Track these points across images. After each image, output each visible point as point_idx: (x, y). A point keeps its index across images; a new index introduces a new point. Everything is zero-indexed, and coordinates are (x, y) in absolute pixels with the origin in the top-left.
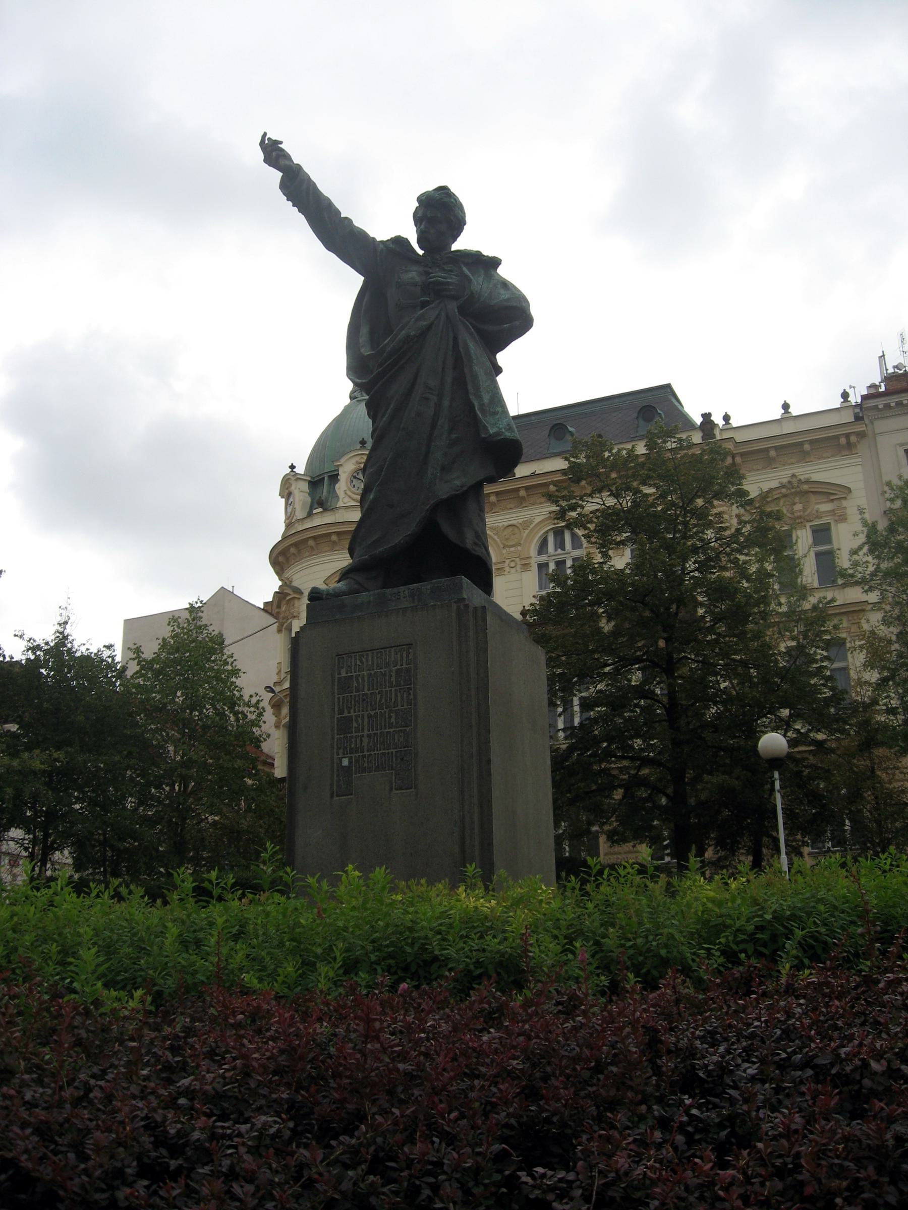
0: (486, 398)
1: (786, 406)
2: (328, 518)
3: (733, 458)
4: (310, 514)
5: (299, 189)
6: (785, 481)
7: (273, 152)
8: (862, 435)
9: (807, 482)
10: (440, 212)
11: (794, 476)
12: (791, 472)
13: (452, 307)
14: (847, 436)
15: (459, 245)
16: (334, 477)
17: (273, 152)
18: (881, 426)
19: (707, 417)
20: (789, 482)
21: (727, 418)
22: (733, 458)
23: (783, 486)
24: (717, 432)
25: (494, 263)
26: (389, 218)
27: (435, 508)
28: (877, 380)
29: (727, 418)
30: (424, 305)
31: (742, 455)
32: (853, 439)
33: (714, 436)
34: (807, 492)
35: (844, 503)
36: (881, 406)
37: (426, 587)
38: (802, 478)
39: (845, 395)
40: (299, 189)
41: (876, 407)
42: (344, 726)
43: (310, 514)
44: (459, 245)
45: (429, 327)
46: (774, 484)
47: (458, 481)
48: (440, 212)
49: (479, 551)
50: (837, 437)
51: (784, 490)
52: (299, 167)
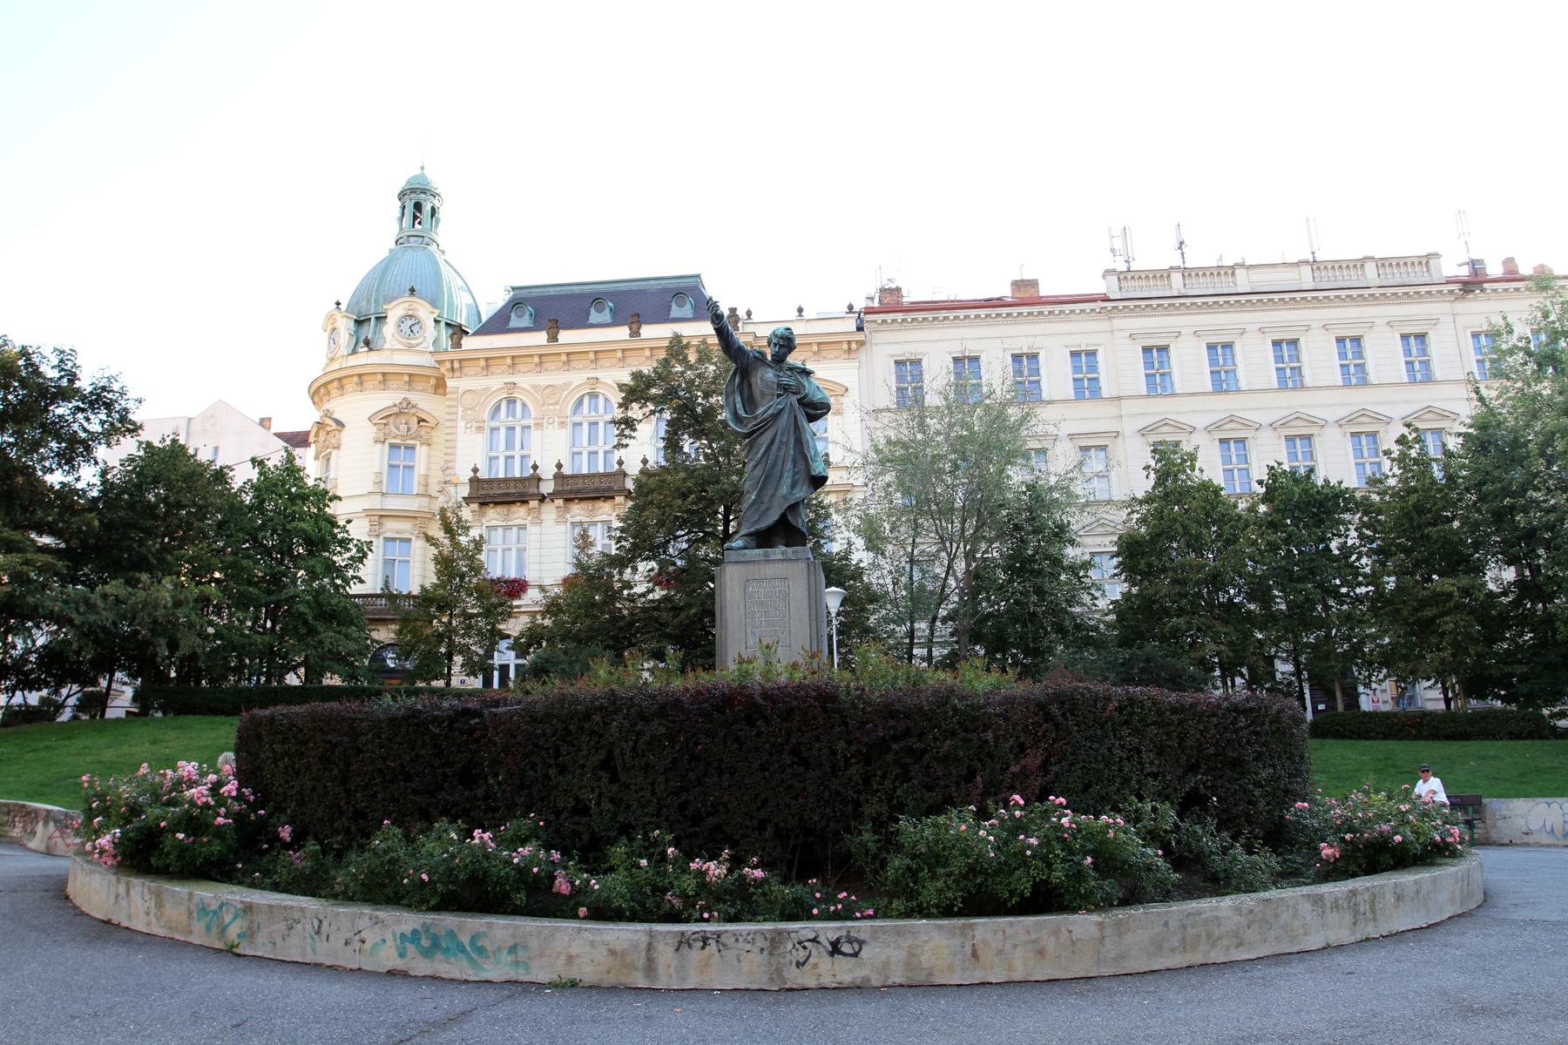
1: (800, 310)
2: (374, 358)
4: (354, 352)
8: (861, 344)
13: (794, 399)
16: (381, 319)
18: (878, 338)
19: (733, 310)
21: (749, 314)
29: (749, 314)
32: (854, 346)
37: (790, 550)
39: (851, 308)
43: (354, 352)
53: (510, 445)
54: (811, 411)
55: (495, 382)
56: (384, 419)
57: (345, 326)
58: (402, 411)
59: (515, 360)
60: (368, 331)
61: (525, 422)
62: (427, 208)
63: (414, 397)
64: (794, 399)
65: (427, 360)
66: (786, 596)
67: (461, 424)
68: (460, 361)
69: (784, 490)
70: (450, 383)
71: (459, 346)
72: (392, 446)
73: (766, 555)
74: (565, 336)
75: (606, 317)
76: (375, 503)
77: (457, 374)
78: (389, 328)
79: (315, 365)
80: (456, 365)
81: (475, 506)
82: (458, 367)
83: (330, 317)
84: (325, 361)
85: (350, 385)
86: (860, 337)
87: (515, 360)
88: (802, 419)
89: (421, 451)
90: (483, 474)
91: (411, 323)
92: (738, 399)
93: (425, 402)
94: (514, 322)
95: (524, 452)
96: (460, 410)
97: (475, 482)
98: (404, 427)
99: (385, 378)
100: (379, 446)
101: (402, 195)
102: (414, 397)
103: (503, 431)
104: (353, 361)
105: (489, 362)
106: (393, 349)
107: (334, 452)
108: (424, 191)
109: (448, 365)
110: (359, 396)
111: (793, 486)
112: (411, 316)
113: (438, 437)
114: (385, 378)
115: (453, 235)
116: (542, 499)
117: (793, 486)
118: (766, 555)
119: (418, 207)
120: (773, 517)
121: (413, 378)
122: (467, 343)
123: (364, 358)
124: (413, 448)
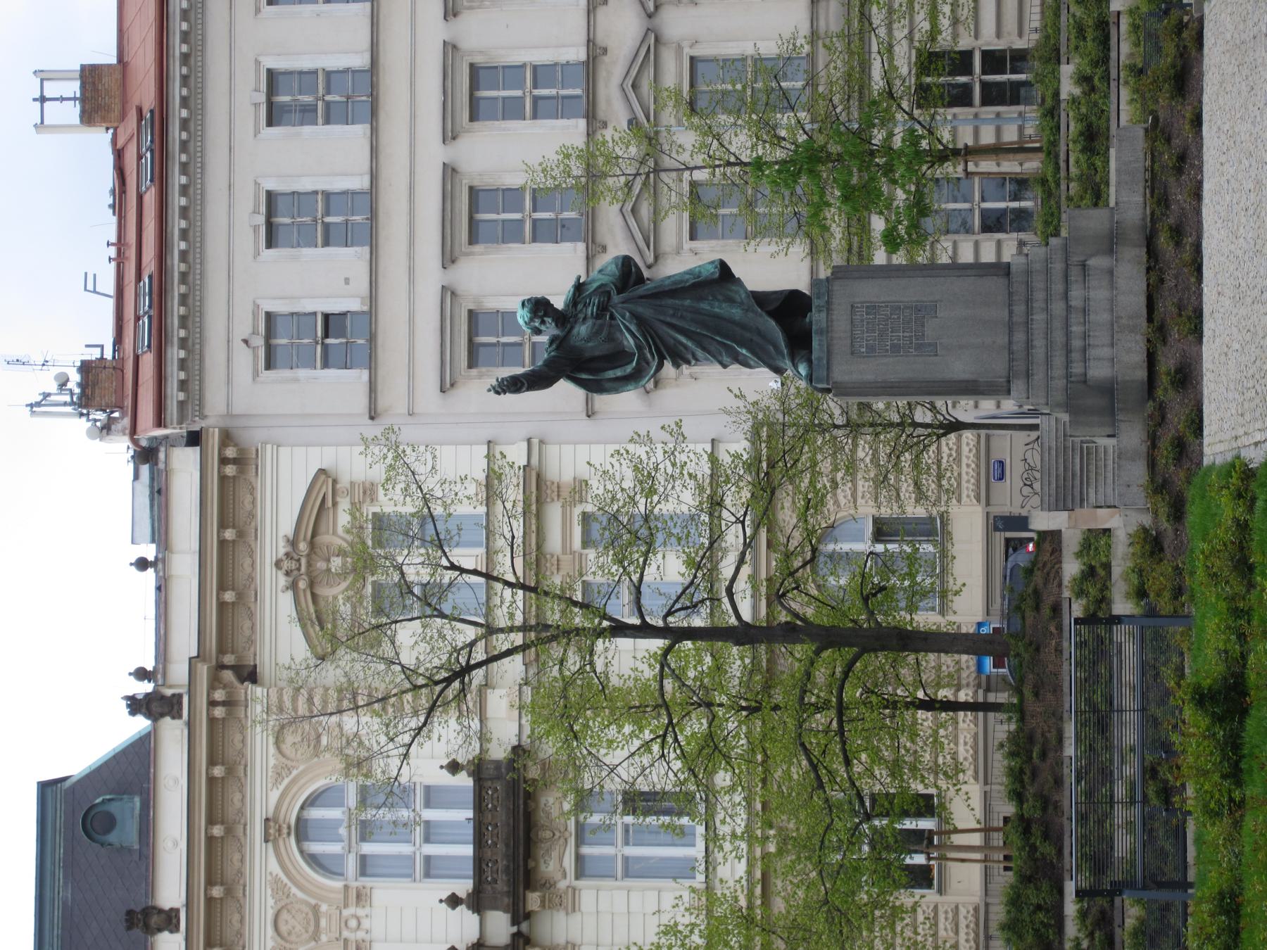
3: (222, 667)
6: (283, 580)
8: (227, 438)
9: (293, 543)
11: (278, 564)
12: (269, 569)
14: (224, 461)
19: (136, 705)
20: (287, 574)
21: (141, 674)
22: (222, 667)
23: (293, 586)
28: (83, 424)
29: (141, 674)
30: (612, 317)
31: (221, 650)
32: (230, 452)
34: (312, 544)
35: (344, 483)
36: (181, 396)
38: (282, 551)
41: (182, 404)
42: (896, 349)
46: (287, 600)
50: (223, 479)
51: (302, 585)
64: (616, 298)
66: (872, 308)
69: (736, 313)
73: (820, 332)
86: (214, 440)
88: (641, 290)
92: (610, 374)
117: (731, 300)
118: (820, 332)
120: (772, 326)
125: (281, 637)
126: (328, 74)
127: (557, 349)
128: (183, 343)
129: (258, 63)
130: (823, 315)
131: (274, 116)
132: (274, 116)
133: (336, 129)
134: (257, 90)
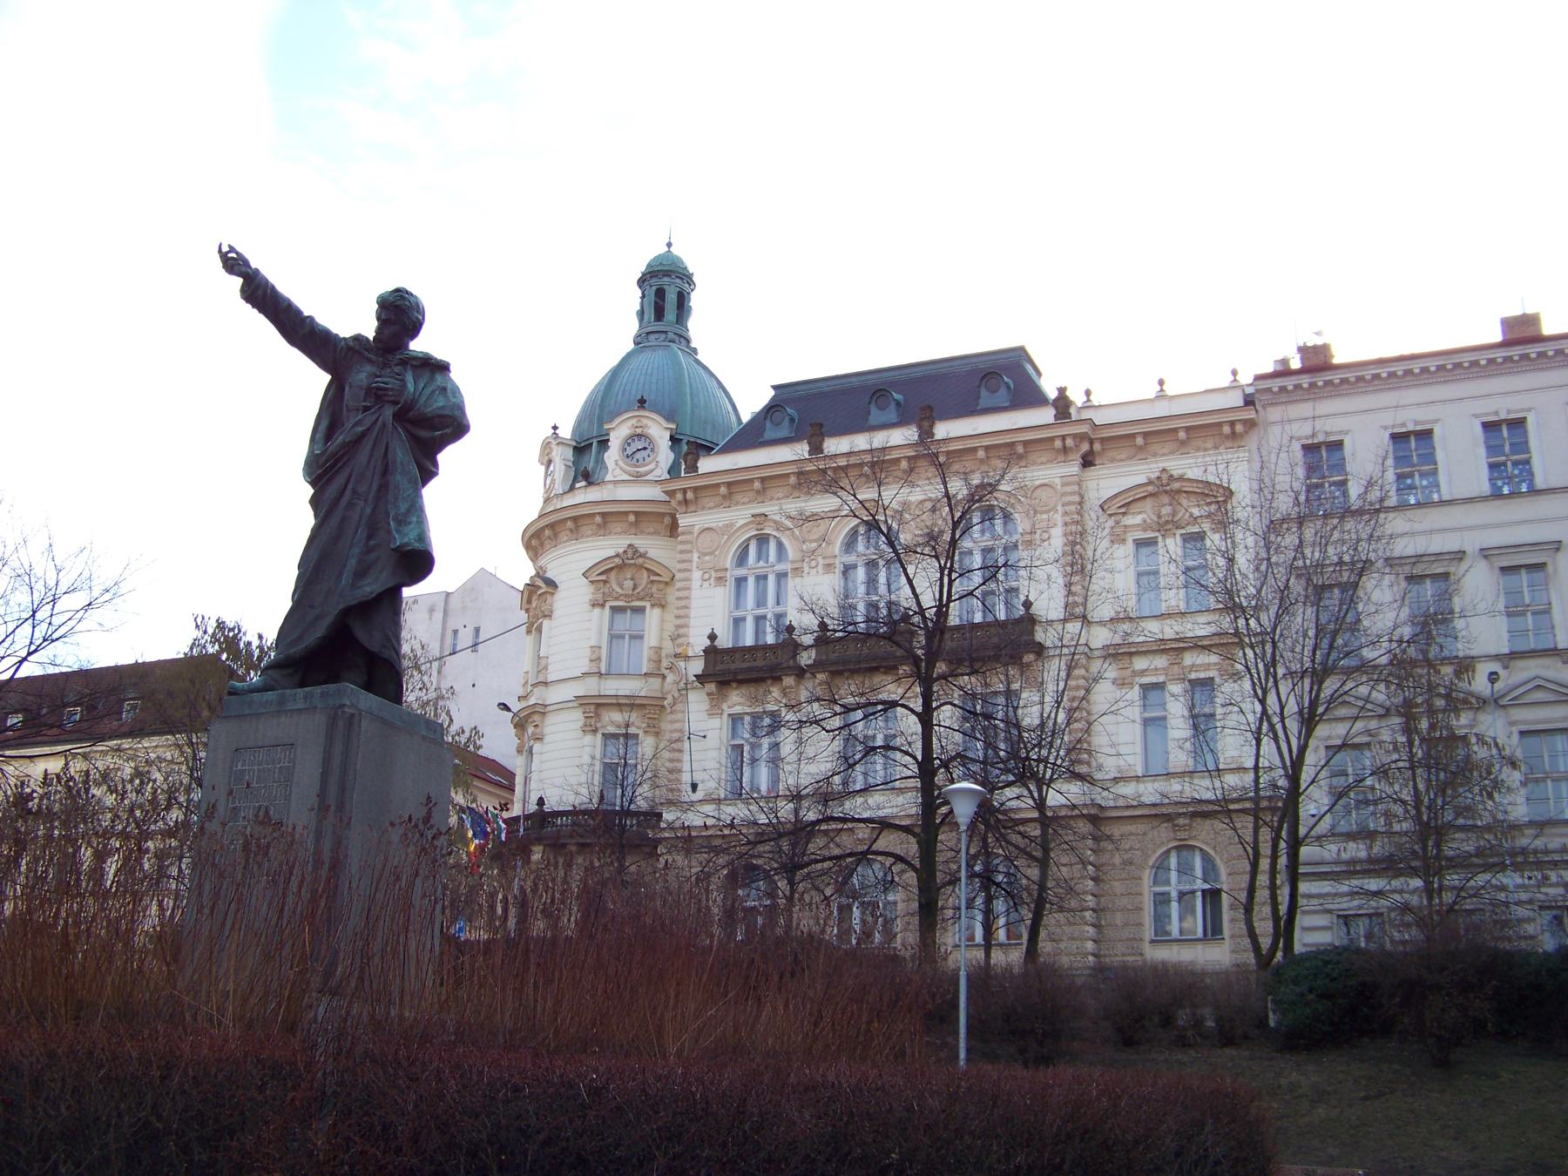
0: (403, 507)
2: (594, 494)
3: (1092, 443)
4: (572, 488)
5: (260, 294)
6: (1153, 476)
7: (233, 263)
8: (1250, 424)
9: (1181, 478)
10: (400, 314)
11: (1164, 470)
12: (1162, 465)
13: (389, 412)
14: (1232, 424)
15: (417, 345)
16: (604, 444)
17: (233, 263)
18: (1274, 414)
19: (1062, 391)
22: (1092, 443)
23: (1150, 483)
24: (1072, 411)
25: (444, 367)
26: (354, 319)
27: (347, 612)
30: (366, 409)
31: (1103, 440)
32: (1239, 428)
33: (1069, 416)
34: (1179, 492)
36: (1276, 390)
38: (1175, 473)
40: (260, 294)
41: (1269, 390)
43: (572, 488)
44: (417, 345)
45: (363, 435)
46: (1142, 479)
47: (371, 587)
48: (400, 314)
49: (386, 654)
50: (1220, 425)
51: (1150, 488)
52: (257, 271)
53: (761, 601)
54: (424, 434)
55: (740, 515)
56: (602, 575)
57: (563, 456)
58: (628, 562)
59: (767, 482)
60: (589, 462)
61: (780, 567)
62: (671, 297)
63: (643, 543)
65: (654, 493)
67: (697, 575)
68: (695, 489)
70: (683, 521)
71: (695, 469)
72: (614, 609)
73: (282, 701)
74: (836, 445)
75: (892, 415)
76: (591, 687)
77: (692, 508)
78: (612, 456)
79: (530, 508)
80: (690, 495)
81: (712, 687)
82: (693, 498)
83: (546, 446)
84: (541, 501)
85: (563, 536)
87: (767, 482)
89: (653, 616)
90: (725, 641)
91: (639, 444)
93: (655, 548)
94: (769, 434)
95: (779, 609)
96: (695, 556)
97: (712, 652)
98: (629, 584)
99: (606, 519)
100: (597, 610)
101: (642, 282)
102: (643, 543)
103: (751, 581)
104: (569, 501)
105: (733, 488)
106: (621, 483)
107: (546, 623)
108: (667, 273)
109: (679, 496)
110: (574, 546)
111: (361, 573)
112: (640, 436)
113: (672, 595)
114: (606, 519)
115: (705, 327)
116: (800, 673)
119: (660, 293)
121: (640, 517)
122: (706, 464)
123: (585, 495)
124: (641, 610)
125: (1110, 480)
126: (1528, 462)
127: (350, 349)
128: (1312, 385)
129: (1529, 410)
130: (300, 705)
131: (1490, 427)
132: (1490, 427)
133: (1485, 472)
134: (1509, 412)
